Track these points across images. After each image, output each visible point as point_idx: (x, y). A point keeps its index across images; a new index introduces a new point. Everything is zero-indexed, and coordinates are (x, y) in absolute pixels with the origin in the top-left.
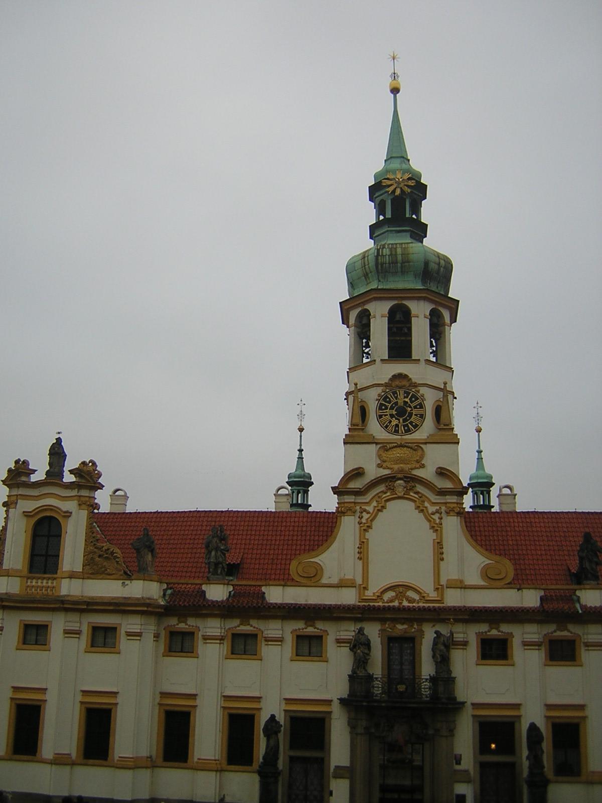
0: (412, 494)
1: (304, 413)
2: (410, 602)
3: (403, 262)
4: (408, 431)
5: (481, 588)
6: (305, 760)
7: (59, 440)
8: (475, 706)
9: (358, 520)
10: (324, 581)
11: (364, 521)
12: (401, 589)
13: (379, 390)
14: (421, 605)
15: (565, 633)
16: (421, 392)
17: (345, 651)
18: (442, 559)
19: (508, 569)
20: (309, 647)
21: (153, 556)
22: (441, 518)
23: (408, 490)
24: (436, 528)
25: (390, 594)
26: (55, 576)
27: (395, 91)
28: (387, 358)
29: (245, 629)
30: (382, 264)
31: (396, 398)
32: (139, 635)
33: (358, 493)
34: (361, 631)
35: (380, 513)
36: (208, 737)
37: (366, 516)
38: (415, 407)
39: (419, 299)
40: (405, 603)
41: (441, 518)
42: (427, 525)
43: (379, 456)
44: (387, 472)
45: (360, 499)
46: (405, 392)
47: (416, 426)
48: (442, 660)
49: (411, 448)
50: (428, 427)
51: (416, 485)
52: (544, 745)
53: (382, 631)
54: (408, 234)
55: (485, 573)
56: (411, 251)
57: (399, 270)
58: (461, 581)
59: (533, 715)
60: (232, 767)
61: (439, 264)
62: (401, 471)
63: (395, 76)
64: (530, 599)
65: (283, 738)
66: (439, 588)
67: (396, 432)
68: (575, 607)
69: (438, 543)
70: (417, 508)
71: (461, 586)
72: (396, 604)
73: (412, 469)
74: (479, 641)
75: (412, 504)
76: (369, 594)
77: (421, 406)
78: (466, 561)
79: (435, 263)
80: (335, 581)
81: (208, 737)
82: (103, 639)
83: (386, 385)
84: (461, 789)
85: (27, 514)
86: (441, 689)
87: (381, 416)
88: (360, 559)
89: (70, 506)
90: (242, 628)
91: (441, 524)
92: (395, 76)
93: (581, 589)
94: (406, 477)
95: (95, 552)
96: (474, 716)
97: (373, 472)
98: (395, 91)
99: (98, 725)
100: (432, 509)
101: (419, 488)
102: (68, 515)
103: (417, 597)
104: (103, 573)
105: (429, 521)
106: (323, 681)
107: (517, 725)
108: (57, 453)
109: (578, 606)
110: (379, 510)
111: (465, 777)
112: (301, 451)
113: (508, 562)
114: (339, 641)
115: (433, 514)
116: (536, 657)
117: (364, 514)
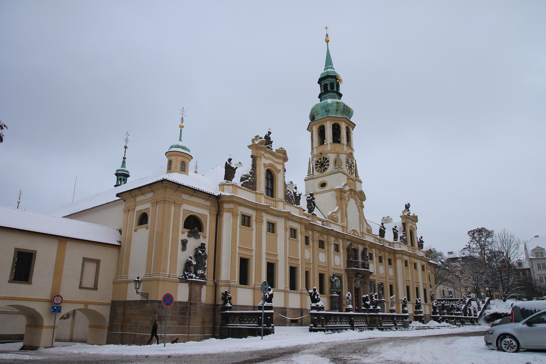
1: (128, 139)
7: (270, 133)
12: (354, 230)
17: (345, 251)
20: (337, 249)
24: (359, 211)
25: (352, 232)
27: (327, 41)
29: (322, 239)
33: (345, 192)
63: (327, 35)
85: (265, 165)
89: (280, 167)
92: (327, 35)
98: (327, 41)
108: (267, 137)
112: (124, 158)
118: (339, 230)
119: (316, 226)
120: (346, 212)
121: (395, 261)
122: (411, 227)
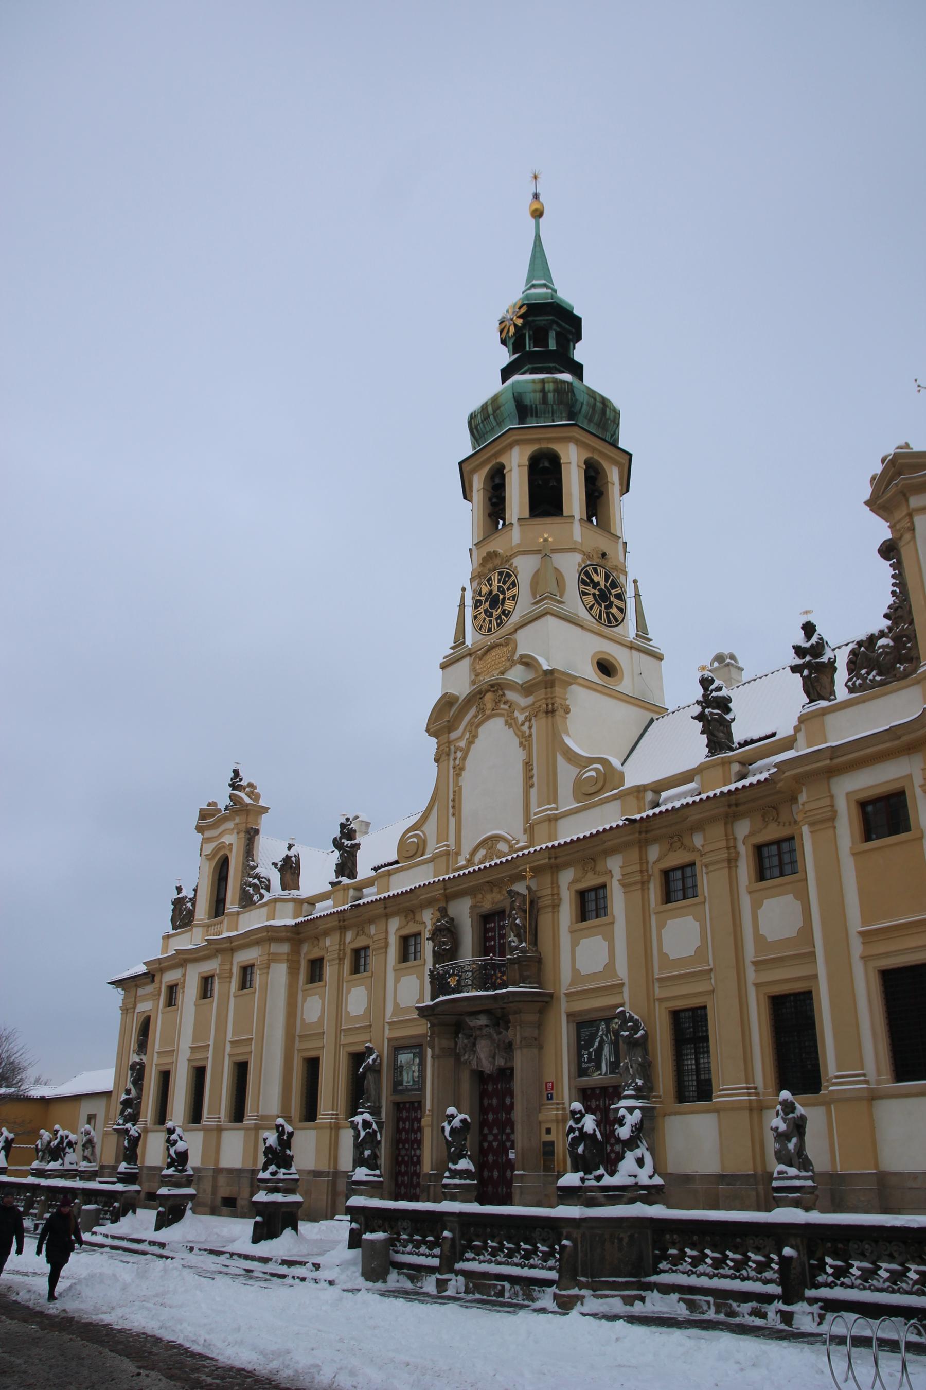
0: (502, 706)
3: (494, 412)
5: (575, 813)
7: (236, 773)
9: (451, 763)
11: (457, 762)
12: (490, 842)
18: (532, 786)
20: (408, 947)
22: (530, 728)
23: (497, 703)
25: (482, 852)
27: (538, 214)
30: (476, 428)
35: (473, 746)
39: (510, 446)
41: (530, 728)
43: (473, 669)
46: (500, 574)
49: (501, 645)
51: (507, 692)
53: (472, 907)
57: (494, 424)
63: (536, 196)
66: (530, 830)
69: (527, 763)
73: (503, 673)
74: (573, 893)
79: (535, 391)
88: (453, 815)
91: (530, 736)
92: (536, 196)
94: (492, 686)
96: (569, 1015)
98: (538, 214)
100: (521, 717)
101: (511, 695)
105: (518, 736)
110: (471, 743)
115: (523, 724)
119: (320, 922)
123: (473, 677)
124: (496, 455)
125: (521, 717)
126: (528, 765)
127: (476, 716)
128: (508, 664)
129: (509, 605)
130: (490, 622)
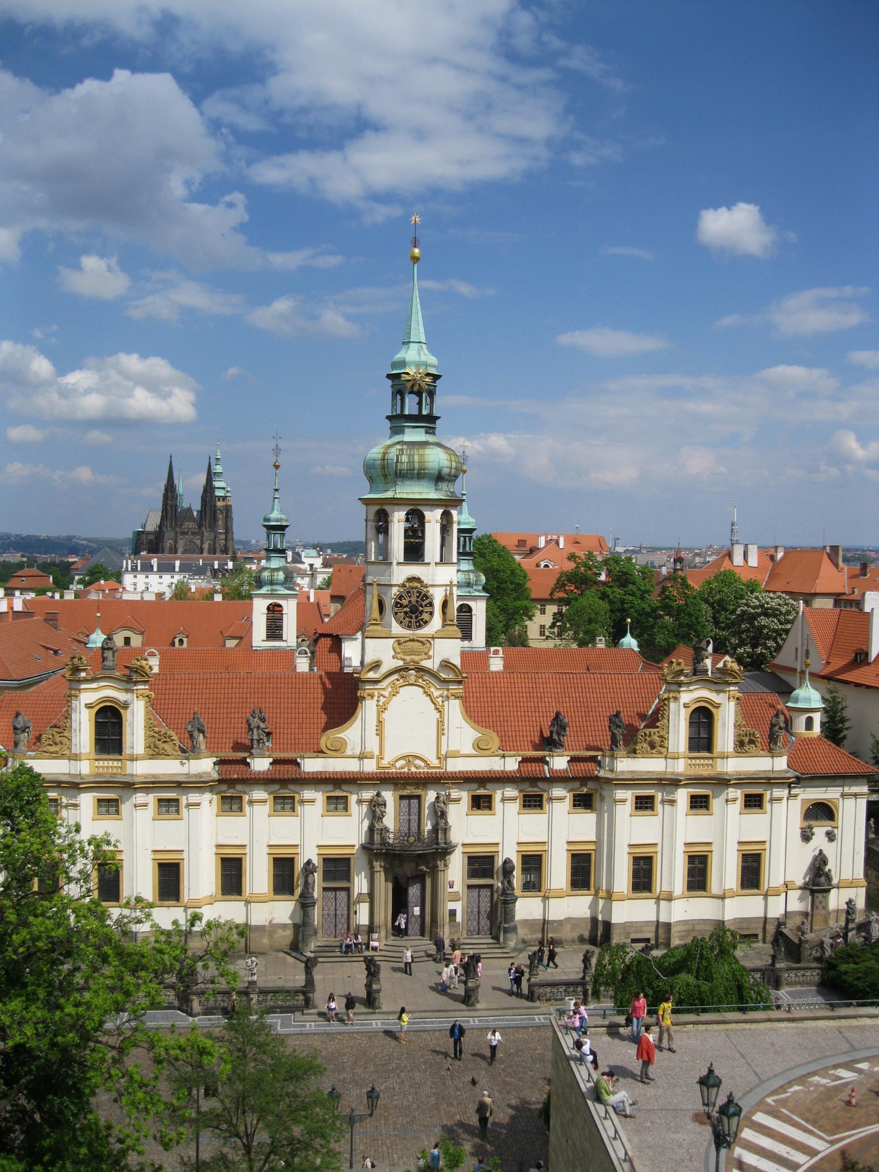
0: (420, 681)
2: (417, 768)
3: (419, 470)
4: (419, 627)
6: (335, 889)
8: (463, 845)
10: (349, 752)
11: (381, 703)
12: (409, 758)
13: (395, 590)
14: (426, 770)
15: (536, 789)
16: (431, 592)
17: (365, 808)
18: (443, 734)
19: (495, 742)
20: (337, 804)
21: (204, 737)
26: (121, 757)
28: (402, 561)
30: (401, 470)
31: (410, 597)
32: (198, 804)
33: (376, 682)
34: (378, 795)
36: (258, 876)
37: (382, 699)
38: (426, 606)
40: (413, 769)
42: (433, 706)
44: (401, 663)
45: (379, 686)
47: (426, 622)
48: (440, 815)
50: (436, 623)
52: (515, 873)
54: (423, 430)
55: (477, 746)
56: (427, 458)
58: (459, 752)
59: (510, 852)
60: (278, 897)
61: (451, 468)
62: (413, 662)
64: (511, 765)
65: (317, 877)
67: (409, 627)
68: (544, 771)
70: (425, 692)
71: (456, 755)
72: (406, 770)
75: (422, 690)
76: (384, 763)
77: (431, 604)
78: (462, 735)
80: (357, 752)
81: (258, 876)
82: (169, 806)
83: (403, 586)
84: (451, 906)
85: (89, 706)
86: (440, 835)
87: (396, 613)
88: (377, 735)
90: (282, 791)
93: (549, 756)
95: (154, 737)
97: (389, 663)
99: (170, 878)
102: (126, 706)
103: (422, 764)
104: (163, 754)
106: (347, 831)
107: (496, 858)
109: (546, 767)
111: (455, 898)
113: (494, 735)
114: (360, 802)
116: (514, 807)
117: (382, 698)
118: (349, 766)
120: (380, 723)
121: (602, 799)
122: (698, 700)
123: (393, 653)
124: (418, 505)
125: (436, 693)
126: (440, 723)
127: (398, 680)
128: (426, 657)
129: (425, 616)
130: (410, 622)
